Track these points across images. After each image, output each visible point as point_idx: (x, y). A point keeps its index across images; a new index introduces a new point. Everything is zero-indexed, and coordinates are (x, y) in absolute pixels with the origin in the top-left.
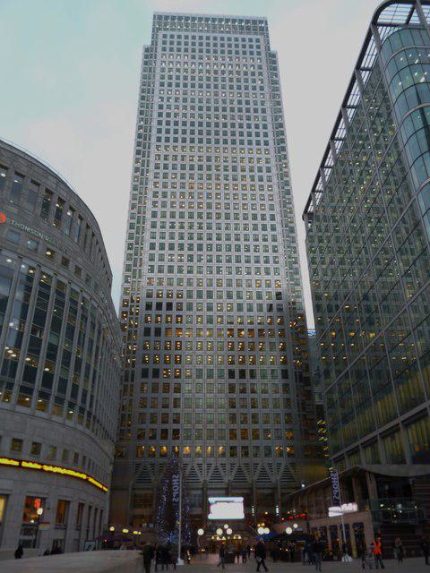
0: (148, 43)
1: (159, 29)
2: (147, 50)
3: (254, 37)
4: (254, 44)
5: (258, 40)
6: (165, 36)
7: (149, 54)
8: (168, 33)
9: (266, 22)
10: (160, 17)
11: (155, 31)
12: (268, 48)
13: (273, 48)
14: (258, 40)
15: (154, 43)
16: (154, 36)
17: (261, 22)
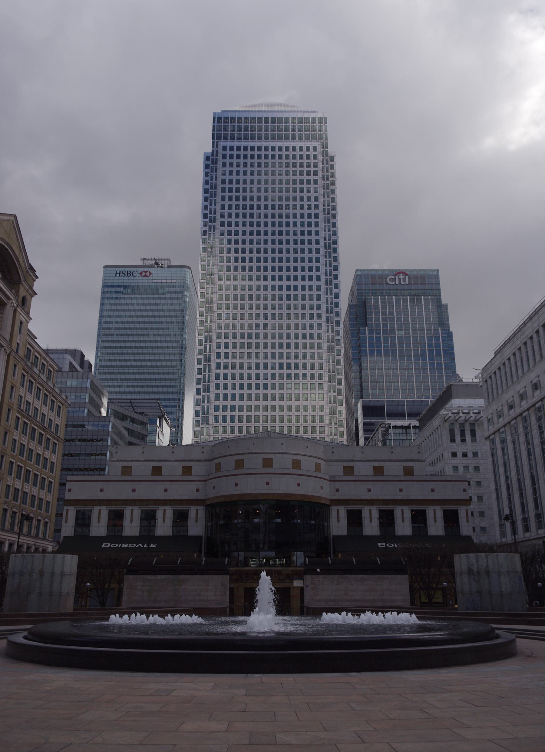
0: (209, 150)
1: (219, 138)
2: (207, 158)
3: (312, 144)
4: (312, 153)
5: (315, 149)
6: (225, 148)
7: (210, 161)
8: (229, 144)
9: (326, 119)
10: (219, 119)
11: (217, 137)
12: (325, 154)
13: (331, 150)
14: (315, 149)
15: (214, 153)
16: (215, 145)
17: (320, 119)
